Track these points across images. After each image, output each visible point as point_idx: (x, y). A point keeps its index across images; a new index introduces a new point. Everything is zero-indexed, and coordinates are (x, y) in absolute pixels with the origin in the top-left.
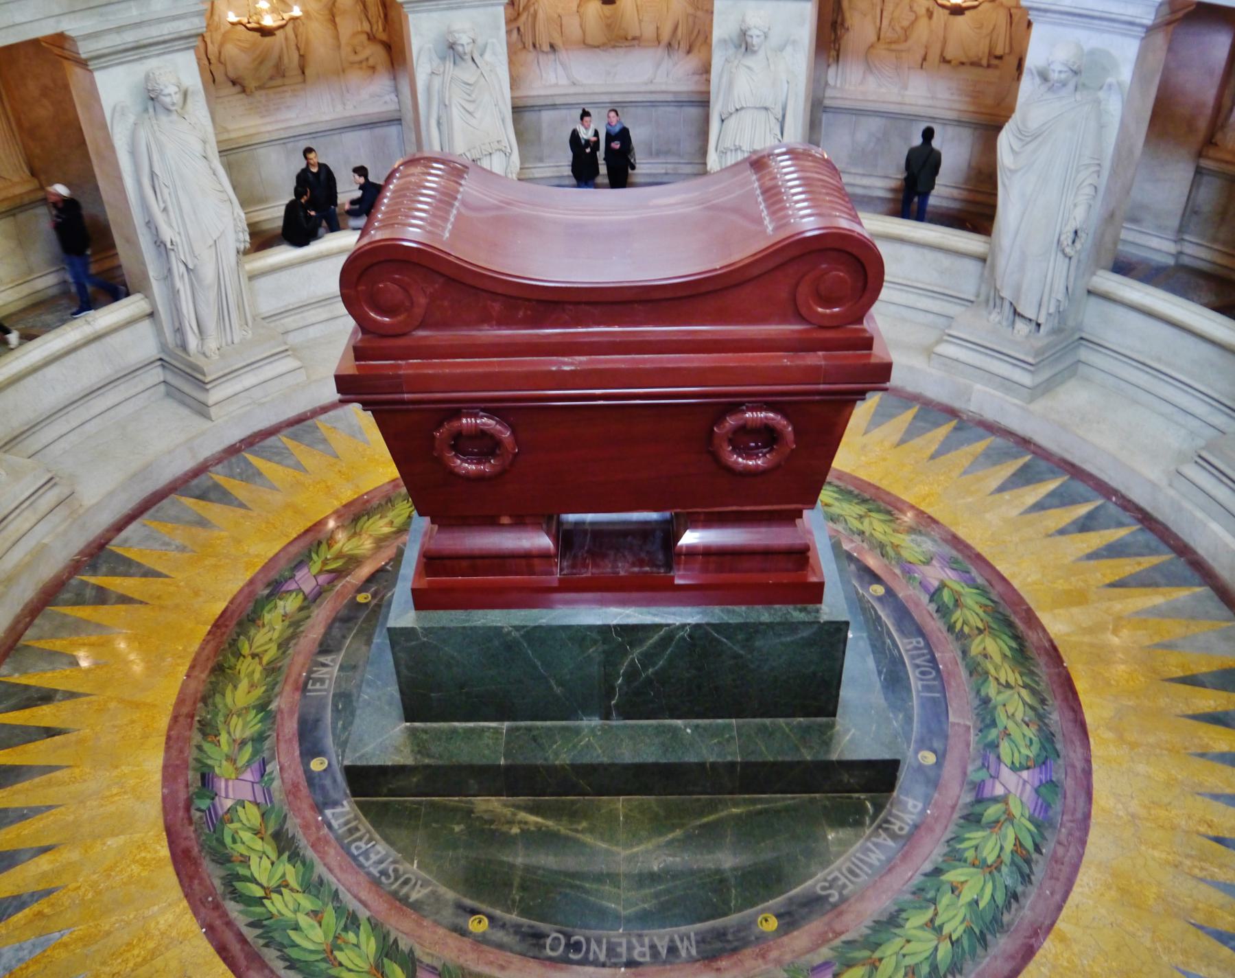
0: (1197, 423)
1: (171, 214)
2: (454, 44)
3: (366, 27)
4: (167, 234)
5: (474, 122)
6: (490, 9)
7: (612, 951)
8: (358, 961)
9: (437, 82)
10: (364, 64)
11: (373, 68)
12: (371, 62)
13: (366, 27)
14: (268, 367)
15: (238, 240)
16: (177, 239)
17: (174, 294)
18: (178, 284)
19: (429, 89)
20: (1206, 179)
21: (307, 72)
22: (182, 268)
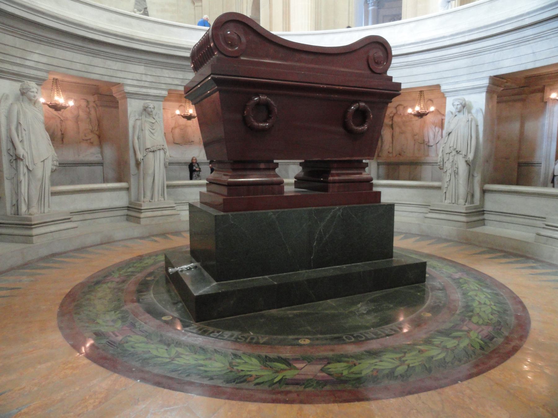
0: (417, 214)
1: (25, 143)
2: (147, 108)
3: (91, 127)
4: (21, 151)
5: (154, 137)
6: (157, 102)
7: (376, 334)
8: (250, 367)
9: (138, 123)
10: (89, 141)
11: (92, 143)
12: (92, 140)
13: (91, 127)
14: (62, 224)
15: (53, 165)
16: (26, 155)
17: (17, 184)
18: (22, 178)
19: (134, 127)
20: (380, 166)
21: (64, 140)
22: (26, 170)
